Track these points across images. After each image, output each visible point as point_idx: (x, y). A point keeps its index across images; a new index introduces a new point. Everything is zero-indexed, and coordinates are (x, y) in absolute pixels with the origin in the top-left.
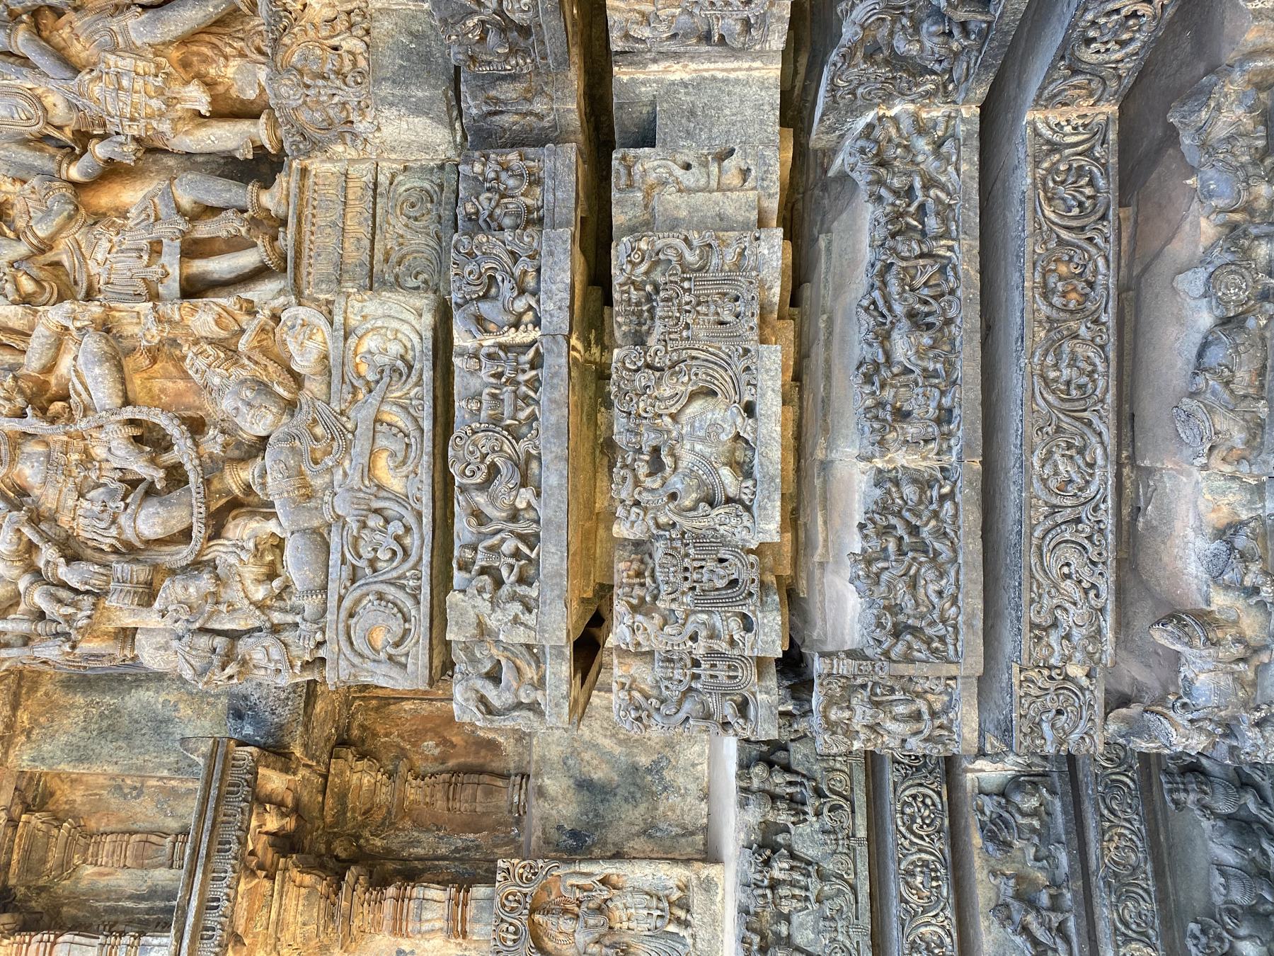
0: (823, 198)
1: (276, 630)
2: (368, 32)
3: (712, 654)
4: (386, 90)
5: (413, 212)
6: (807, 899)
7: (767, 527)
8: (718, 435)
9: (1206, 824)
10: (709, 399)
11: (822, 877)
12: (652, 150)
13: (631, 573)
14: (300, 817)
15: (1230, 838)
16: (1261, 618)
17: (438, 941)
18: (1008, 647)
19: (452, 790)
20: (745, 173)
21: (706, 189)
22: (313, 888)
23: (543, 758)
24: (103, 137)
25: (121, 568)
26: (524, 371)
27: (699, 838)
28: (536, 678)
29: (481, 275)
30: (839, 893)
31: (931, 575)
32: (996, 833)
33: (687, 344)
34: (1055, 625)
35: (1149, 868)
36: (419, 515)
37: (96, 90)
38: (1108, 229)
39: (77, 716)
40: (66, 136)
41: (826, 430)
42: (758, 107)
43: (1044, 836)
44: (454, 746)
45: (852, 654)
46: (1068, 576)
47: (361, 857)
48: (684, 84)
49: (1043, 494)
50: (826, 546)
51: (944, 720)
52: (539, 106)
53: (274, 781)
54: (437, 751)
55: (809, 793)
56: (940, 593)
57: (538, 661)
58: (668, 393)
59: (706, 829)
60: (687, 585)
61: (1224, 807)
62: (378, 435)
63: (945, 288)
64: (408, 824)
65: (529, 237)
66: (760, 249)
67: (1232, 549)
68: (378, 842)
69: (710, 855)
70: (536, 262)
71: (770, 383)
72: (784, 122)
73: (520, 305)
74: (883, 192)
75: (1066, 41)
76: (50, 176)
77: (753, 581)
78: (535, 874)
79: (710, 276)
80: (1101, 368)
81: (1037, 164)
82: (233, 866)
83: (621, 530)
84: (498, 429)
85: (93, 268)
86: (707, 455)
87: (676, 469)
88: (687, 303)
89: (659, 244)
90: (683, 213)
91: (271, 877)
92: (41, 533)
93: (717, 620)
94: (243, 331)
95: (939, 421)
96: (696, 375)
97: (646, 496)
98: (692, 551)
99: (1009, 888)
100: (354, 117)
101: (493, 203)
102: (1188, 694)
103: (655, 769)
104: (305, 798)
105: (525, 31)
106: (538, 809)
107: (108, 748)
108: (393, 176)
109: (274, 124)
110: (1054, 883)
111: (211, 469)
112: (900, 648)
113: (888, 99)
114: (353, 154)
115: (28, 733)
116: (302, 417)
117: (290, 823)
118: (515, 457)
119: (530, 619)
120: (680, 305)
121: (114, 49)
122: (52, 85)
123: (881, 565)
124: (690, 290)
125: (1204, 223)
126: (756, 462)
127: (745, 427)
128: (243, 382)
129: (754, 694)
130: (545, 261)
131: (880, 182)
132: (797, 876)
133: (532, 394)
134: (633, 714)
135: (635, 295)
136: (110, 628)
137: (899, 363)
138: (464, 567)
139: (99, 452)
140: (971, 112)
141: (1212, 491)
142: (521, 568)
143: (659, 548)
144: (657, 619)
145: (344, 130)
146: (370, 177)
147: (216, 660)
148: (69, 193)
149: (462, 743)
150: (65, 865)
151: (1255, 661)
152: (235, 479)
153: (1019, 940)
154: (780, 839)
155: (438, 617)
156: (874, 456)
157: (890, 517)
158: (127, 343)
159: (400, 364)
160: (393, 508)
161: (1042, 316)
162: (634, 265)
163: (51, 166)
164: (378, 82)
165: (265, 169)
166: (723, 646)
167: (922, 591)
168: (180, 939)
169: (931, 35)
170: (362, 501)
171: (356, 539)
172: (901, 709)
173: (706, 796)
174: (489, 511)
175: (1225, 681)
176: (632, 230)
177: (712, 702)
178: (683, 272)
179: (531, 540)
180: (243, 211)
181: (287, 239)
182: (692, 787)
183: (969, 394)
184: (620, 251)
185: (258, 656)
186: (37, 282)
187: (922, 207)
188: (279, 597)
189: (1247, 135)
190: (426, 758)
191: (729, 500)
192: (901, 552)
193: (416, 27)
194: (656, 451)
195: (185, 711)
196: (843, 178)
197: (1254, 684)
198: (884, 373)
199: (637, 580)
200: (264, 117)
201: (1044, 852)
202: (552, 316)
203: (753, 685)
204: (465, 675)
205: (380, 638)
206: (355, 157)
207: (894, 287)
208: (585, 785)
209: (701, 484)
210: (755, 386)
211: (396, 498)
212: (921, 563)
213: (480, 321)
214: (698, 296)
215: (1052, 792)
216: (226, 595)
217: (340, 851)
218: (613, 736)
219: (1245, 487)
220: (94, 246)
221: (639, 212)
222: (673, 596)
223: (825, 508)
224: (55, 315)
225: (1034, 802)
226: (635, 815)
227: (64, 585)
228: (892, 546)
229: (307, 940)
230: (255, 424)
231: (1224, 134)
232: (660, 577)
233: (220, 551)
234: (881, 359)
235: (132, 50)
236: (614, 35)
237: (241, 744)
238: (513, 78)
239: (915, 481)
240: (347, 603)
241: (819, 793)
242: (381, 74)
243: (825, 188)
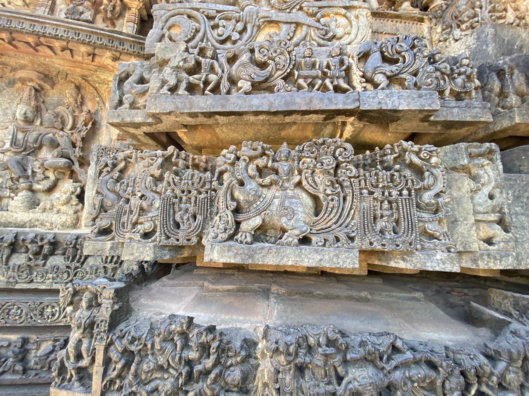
0: (432, 291)
2: (518, 25)
6: (106, 262)
7: (215, 252)
8: (286, 216)
10: (313, 210)
12: (501, 171)
13: (197, 161)
20: (489, 241)
21: (475, 212)
26: (332, 83)
28: (139, 105)
29: (399, 53)
33: (357, 192)
41: (290, 294)
50: (213, 290)
58: (316, 178)
60: (178, 192)
62: (288, 25)
66: (440, 253)
70: (412, 87)
71: (327, 257)
77: (178, 240)
79: (414, 210)
84: (291, 67)
86: (271, 208)
87: (263, 186)
88: (390, 194)
96: (332, 200)
98: (202, 196)
101: (444, 70)
118: (272, 79)
119: (165, 90)
120: (389, 187)
123: (179, 344)
124: (401, 195)
126: (267, 244)
129: (113, 239)
133: (316, 87)
134: (110, 162)
137: (347, 372)
142: (197, 85)
156: (267, 341)
157: (215, 356)
159: (330, 34)
160: (246, 36)
162: (417, 154)
167: (159, 375)
170: (251, 19)
178: (415, 190)
179: (216, 90)
191: (238, 224)
199: (190, 163)
202: (374, 98)
203: (118, 240)
206: (433, 40)
209: (250, 203)
210: (324, 245)
212: (177, 379)
214: (396, 201)
222: (172, 183)
223: (238, 290)
240: (195, 13)
242: (498, 28)
243: (437, 292)
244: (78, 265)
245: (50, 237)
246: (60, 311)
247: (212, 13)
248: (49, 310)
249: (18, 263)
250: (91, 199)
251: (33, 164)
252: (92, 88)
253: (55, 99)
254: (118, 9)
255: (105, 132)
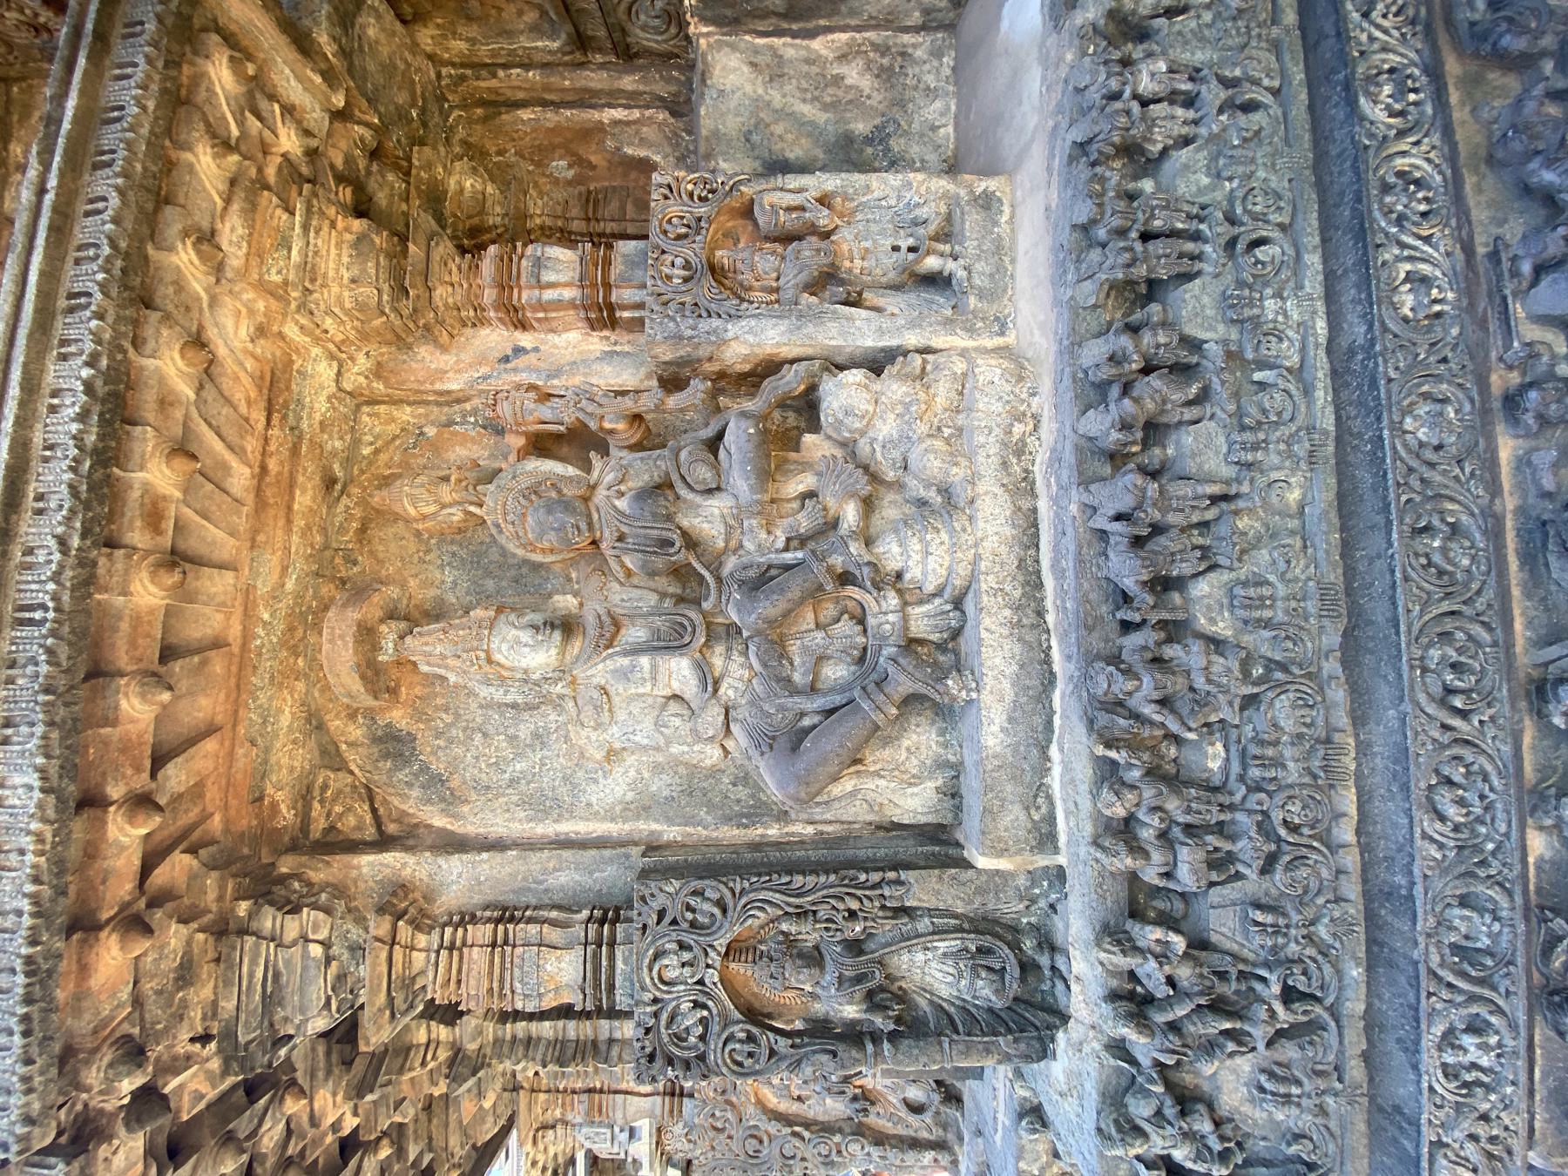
23: (716, 133)
44: (594, 167)
54: (570, 174)
78: (713, 191)
82: (146, 56)
149: (604, 163)
190: (556, 182)
218: (815, 99)
246: (1410, 259)
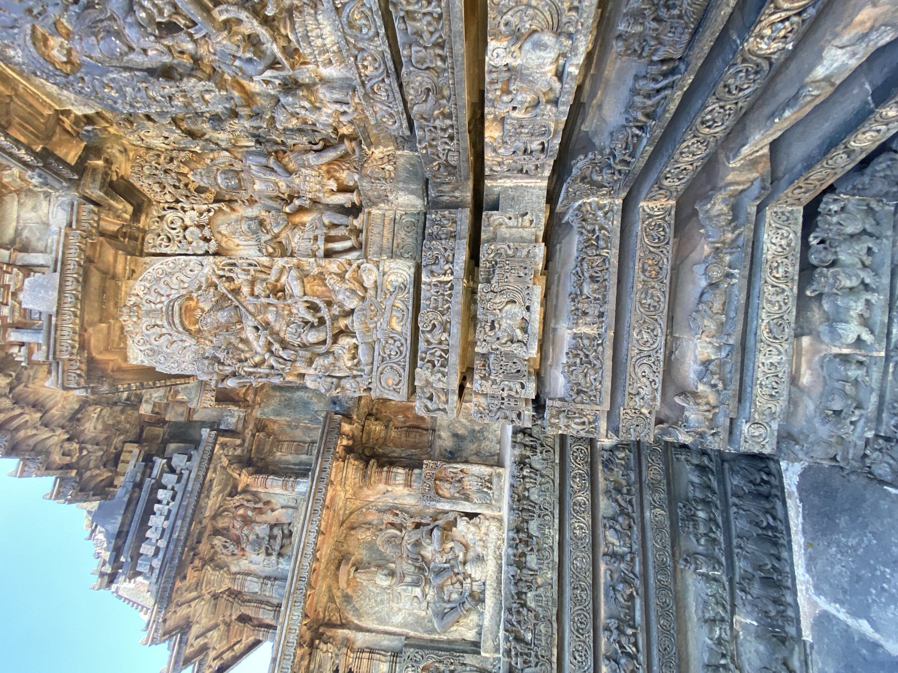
1: (355, 377)
3: (509, 396)
4: (401, 185)
5: (408, 230)
9: (688, 467)
11: (542, 476)
14: (354, 440)
15: (697, 473)
16: (717, 396)
17: (401, 488)
18: (619, 400)
19: (408, 434)
20: (532, 222)
21: (517, 227)
22: (357, 466)
24: (298, 197)
25: (301, 353)
27: (496, 457)
30: (548, 482)
31: (592, 372)
32: (607, 464)
34: (638, 393)
35: (665, 481)
36: (406, 340)
37: (297, 181)
38: (669, 248)
39: (277, 400)
40: (286, 196)
42: (538, 197)
43: (627, 467)
45: (562, 399)
46: (644, 376)
47: (374, 456)
48: (511, 188)
49: (637, 345)
51: (593, 425)
52: (457, 194)
53: (346, 427)
55: (538, 445)
56: (595, 379)
57: (446, 394)
59: (498, 454)
61: (695, 462)
63: (604, 267)
64: (391, 445)
65: (451, 243)
67: (707, 370)
68: (380, 450)
69: (500, 464)
72: (547, 202)
73: (447, 267)
74: (583, 231)
75: (658, 178)
76: (279, 211)
80: (662, 299)
81: (643, 222)
83: (477, 350)
85: (293, 245)
89: (498, 247)
90: (508, 236)
91: (344, 461)
92: (273, 338)
93: (511, 384)
94: (347, 271)
95: (599, 317)
97: (488, 338)
99: (611, 486)
100: (389, 194)
102: (686, 422)
103: (481, 431)
104: (356, 434)
105: (455, 167)
106: (438, 443)
107: (287, 411)
108: (401, 216)
109: (359, 195)
110: (628, 485)
111: (335, 318)
112: (579, 399)
113: (588, 196)
114: (387, 207)
115: (260, 404)
116: (366, 303)
117: (351, 442)
119: (445, 380)
121: (304, 167)
122: (282, 179)
125: (706, 247)
127: (526, 315)
128: (346, 289)
130: (456, 252)
131: (583, 227)
132: (532, 475)
135: (488, 265)
136: (296, 373)
138: (423, 359)
139: (294, 311)
140: (619, 202)
141: (701, 347)
143: (492, 357)
144: (490, 382)
145: (384, 199)
146: (392, 216)
147: (333, 386)
148: (285, 217)
150: (271, 452)
151: (713, 412)
152: (342, 323)
153: (614, 504)
154: (527, 461)
155: (412, 377)
158: (306, 273)
160: (397, 337)
161: (641, 279)
163: (279, 207)
164: (398, 182)
165: (354, 210)
166: (513, 393)
168: (312, 481)
169: (606, 174)
171: (384, 347)
172: (577, 420)
173: (499, 442)
174: (432, 340)
175: (701, 418)
176: (488, 241)
177: (508, 413)
179: (446, 352)
180: (347, 226)
181: (362, 237)
182: (494, 439)
183: (611, 307)
184: (484, 248)
185: (348, 386)
186: (274, 249)
187: (598, 237)
188: (356, 365)
189: (725, 214)
191: (519, 341)
192: (582, 364)
193: (413, 162)
194: (493, 322)
195: (315, 400)
196: (567, 223)
197: (712, 420)
198: (580, 298)
200: (355, 193)
201: (625, 473)
204: (420, 397)
205: (390, 382)
207: (585, 266)
208: (455, 435)
211: (398, 333)
213: (432, 272)
215: (630, 451)
216: (338, 364)
217: (367, 453)
219: (714, 346)
220: (294, 236)
221: (491, 234)
224: (280, 262)
225: (623, 455)
226: (473, 447)
227: (281, 357)
228: (578, 361)
229: (355, 484)
230: (349, 305)
231: (716, 214)
232: (492, 367)
233: (336, 348)
234: (579, 293)
235: (311, 167)
236: (487, 169)
237: (336, 413)
238: (448, 183)
239: (588, 338)
240: (380, 369)
241: (542, 445)
244: (537, 507)
245: (511, 534)
247: (380, 358)
248: (578, 532)
249: (535, 560)
250: (473, 506)
251: (439, 561)
252: (352, 516)
253: (364, 552)
254: (249, 497)
255: (401, 501)
